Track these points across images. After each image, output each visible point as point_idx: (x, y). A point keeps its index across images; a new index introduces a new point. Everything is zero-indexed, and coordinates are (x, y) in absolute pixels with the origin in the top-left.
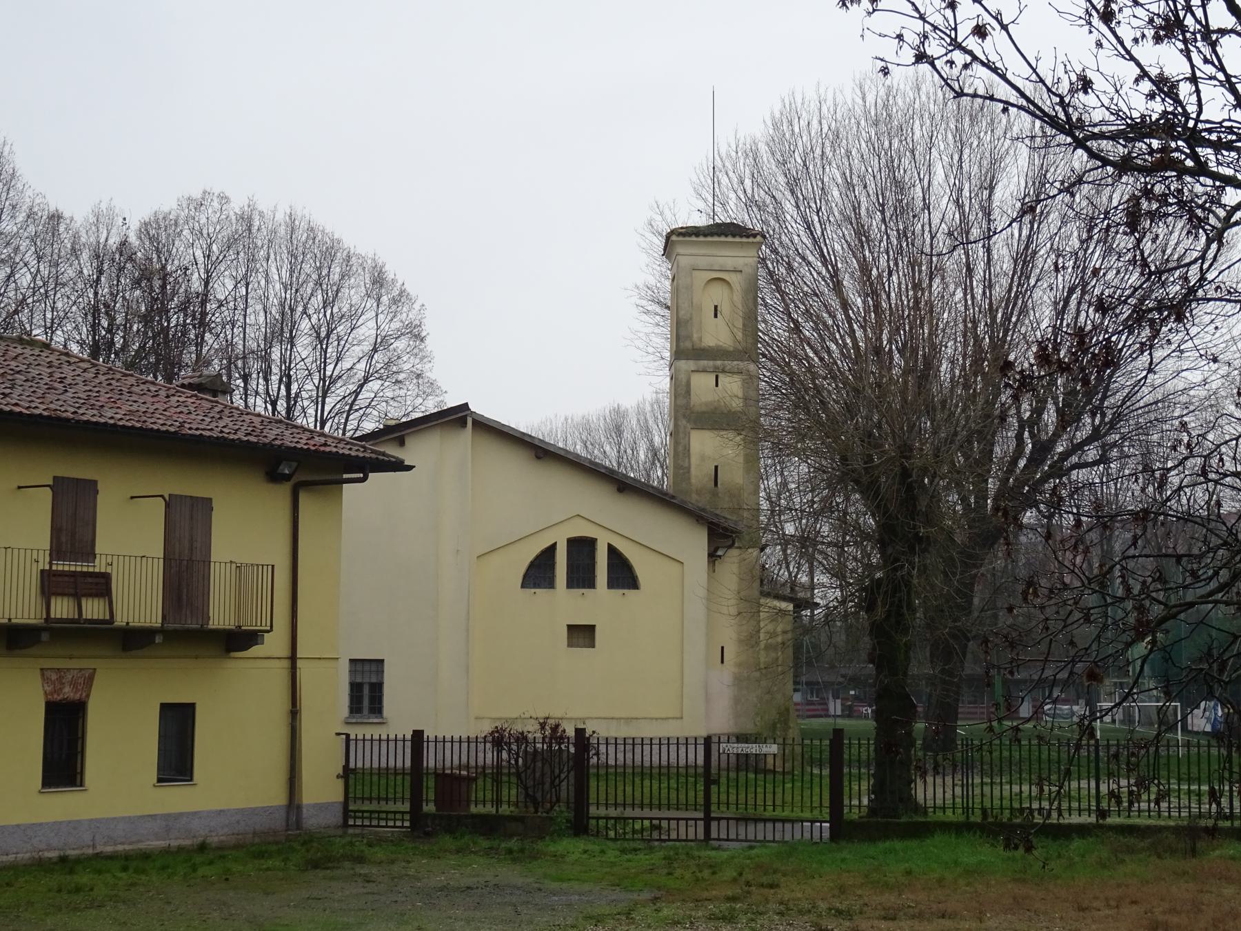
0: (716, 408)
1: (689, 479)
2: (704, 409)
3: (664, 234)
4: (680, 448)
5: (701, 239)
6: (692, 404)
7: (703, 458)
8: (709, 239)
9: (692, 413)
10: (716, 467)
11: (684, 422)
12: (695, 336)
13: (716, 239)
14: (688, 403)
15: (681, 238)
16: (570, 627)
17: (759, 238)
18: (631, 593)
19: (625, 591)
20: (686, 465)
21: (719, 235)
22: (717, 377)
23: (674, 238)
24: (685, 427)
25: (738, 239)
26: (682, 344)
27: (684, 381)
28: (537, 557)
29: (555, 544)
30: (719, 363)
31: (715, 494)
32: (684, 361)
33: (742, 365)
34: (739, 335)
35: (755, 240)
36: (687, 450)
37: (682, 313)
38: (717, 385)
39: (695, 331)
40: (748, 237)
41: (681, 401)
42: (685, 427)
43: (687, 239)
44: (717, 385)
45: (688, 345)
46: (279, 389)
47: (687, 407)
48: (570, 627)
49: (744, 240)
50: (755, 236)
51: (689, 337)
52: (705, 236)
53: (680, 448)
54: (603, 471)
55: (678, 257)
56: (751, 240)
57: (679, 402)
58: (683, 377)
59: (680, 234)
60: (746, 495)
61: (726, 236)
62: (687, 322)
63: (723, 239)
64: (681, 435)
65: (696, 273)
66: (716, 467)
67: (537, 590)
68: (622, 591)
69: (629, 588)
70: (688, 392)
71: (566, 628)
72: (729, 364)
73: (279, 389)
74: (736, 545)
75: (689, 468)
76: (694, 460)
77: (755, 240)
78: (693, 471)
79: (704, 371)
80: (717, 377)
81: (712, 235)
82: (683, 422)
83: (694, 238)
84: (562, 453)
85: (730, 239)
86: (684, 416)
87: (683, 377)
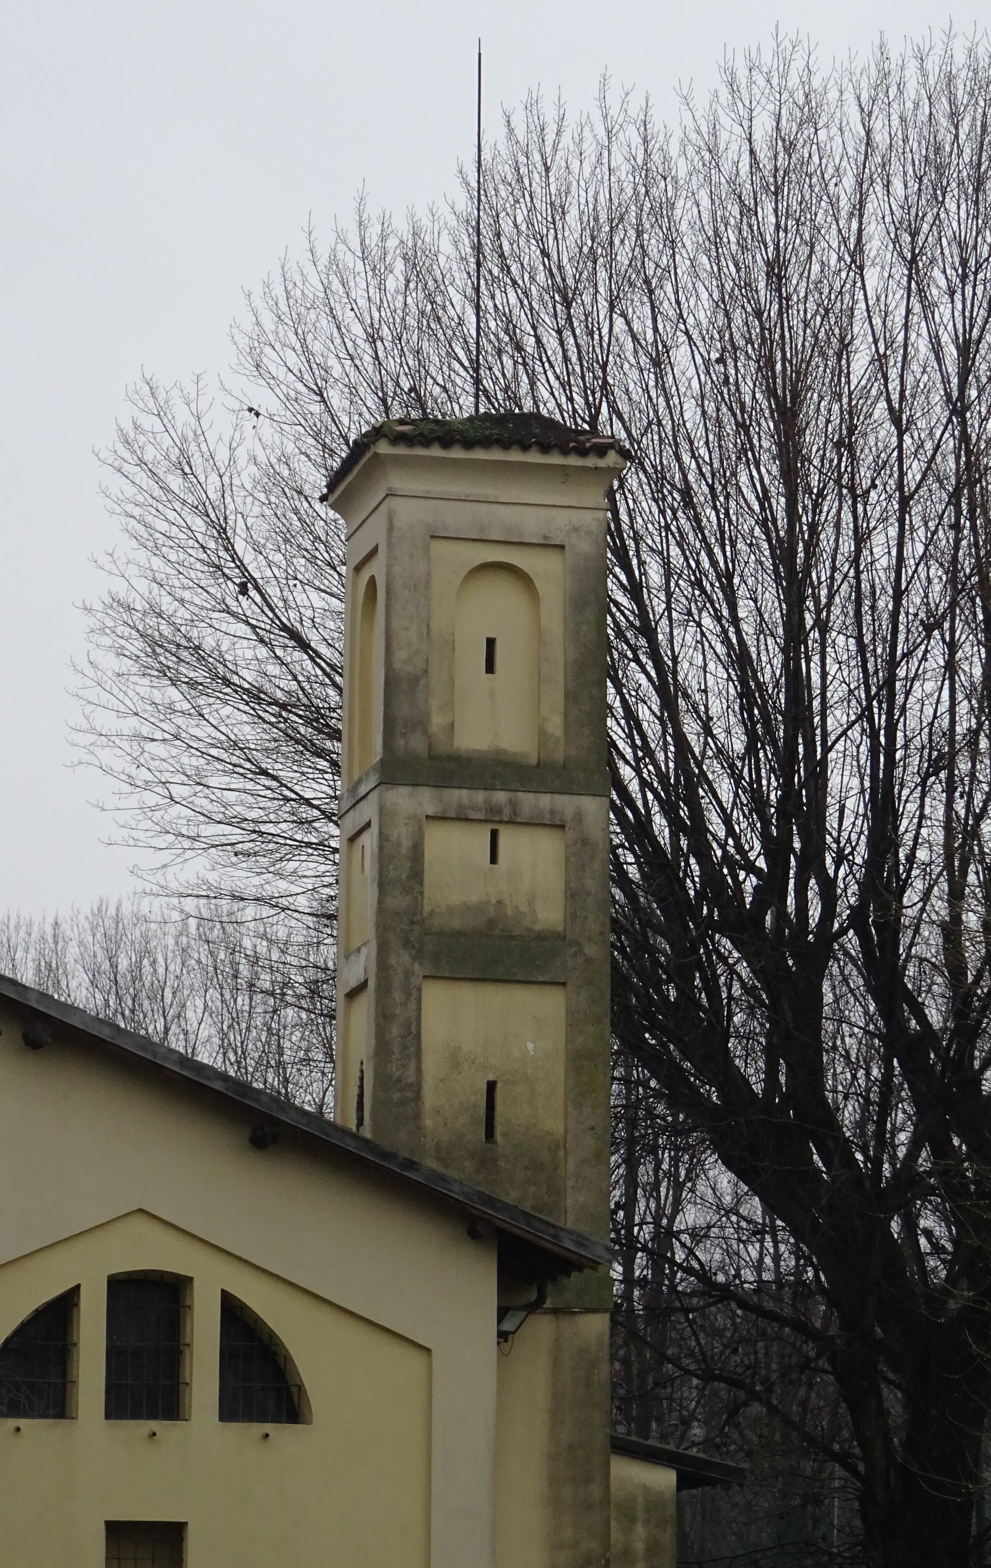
0: (491, 923)
1: (417, 1116)
2: (457, 924)
3: (352, 437)
4: (395, 1030)
5: (457, 453)
6: (427, 909)
7: (455, 1061)
8: (479, 454)
9: (427, 933)
10: (491, 1086)
11: (406, 959)
12: (437, 721)
13: (496, 455)
14: (416, 906)
15: (402, 450)
16: (115, 1530)
17: (612, 458)
18: (283, 1433)
19: (269, 1427)
20: (412, 1079)
21: (506, 445)
22: (494, 835)
23: (383, 448)
24: (408, 974)
25: (555, 459)
26: (401, 742)
27: (406, 843)
28: (23, 1327)
29: (76, 1290)
30: (501, 797)
31: (486, 1161)
32: (403, 790)
33: (566, 804)
34: (555, 725)
35: (602, 463)
36: (413, 1035)
37: (401, 655)
38: (494, 859)
39: (435, 703)
40: (582, 452)
41: (397, 901)
42: (408, 974)
43: (420, 451)
44: (494, 859)
45: (417, 743)
46: (712, 267)
47: (414, 915)
48: (115, 1530)
49: (573, 461)
50: (601, 451)
51: (421, 724)
52: (469, 444)
53: (395, 1030)
54: (217, 1086)
55: (394, 503)
56: (591, 461)
57: (391, 902)
58: (402, 833)
59: (399, 439)
60: (571, 1166)
61: (525, 448)
62: (414, 681)
63: (515, 456)
64: (398, 995)
65: (439, 548)
66: (491, 1086)
67: (23, 1423)
68: (258, 1428)
69: (277, 1419)
70: (417, 874)
71: (102, 1531)
72: (530, 802)
73: (712, 267)
74: (548, 1304)
75: (417, 1088)
76: (432, 1066)
77: (602, 463)
78: (430, 1097)
79: (462, 818)
80: (494, 835)
81: (486, 443)
82: (401, 959)
83: (436, 452)
84: (105, 1033)
85: (534, 457)
86: (407, 943)
87: (402, 833)
